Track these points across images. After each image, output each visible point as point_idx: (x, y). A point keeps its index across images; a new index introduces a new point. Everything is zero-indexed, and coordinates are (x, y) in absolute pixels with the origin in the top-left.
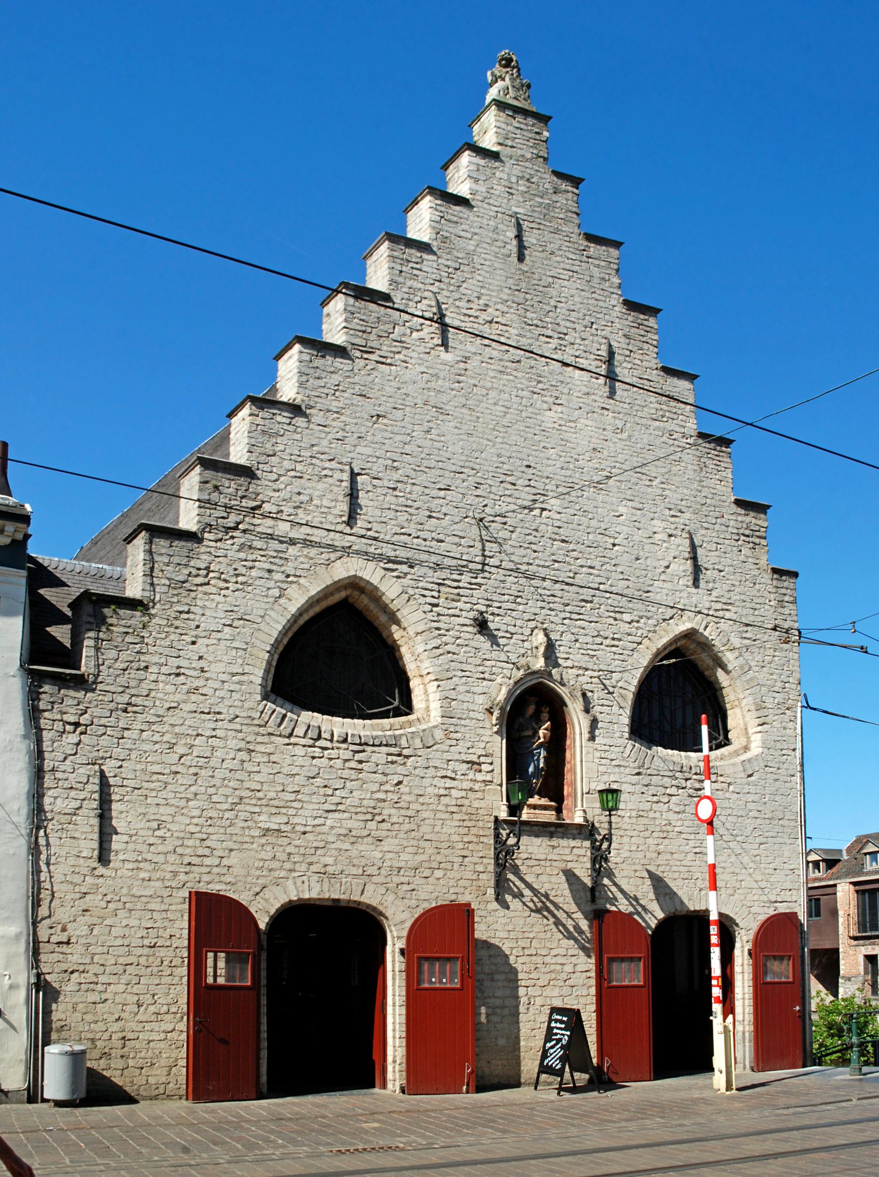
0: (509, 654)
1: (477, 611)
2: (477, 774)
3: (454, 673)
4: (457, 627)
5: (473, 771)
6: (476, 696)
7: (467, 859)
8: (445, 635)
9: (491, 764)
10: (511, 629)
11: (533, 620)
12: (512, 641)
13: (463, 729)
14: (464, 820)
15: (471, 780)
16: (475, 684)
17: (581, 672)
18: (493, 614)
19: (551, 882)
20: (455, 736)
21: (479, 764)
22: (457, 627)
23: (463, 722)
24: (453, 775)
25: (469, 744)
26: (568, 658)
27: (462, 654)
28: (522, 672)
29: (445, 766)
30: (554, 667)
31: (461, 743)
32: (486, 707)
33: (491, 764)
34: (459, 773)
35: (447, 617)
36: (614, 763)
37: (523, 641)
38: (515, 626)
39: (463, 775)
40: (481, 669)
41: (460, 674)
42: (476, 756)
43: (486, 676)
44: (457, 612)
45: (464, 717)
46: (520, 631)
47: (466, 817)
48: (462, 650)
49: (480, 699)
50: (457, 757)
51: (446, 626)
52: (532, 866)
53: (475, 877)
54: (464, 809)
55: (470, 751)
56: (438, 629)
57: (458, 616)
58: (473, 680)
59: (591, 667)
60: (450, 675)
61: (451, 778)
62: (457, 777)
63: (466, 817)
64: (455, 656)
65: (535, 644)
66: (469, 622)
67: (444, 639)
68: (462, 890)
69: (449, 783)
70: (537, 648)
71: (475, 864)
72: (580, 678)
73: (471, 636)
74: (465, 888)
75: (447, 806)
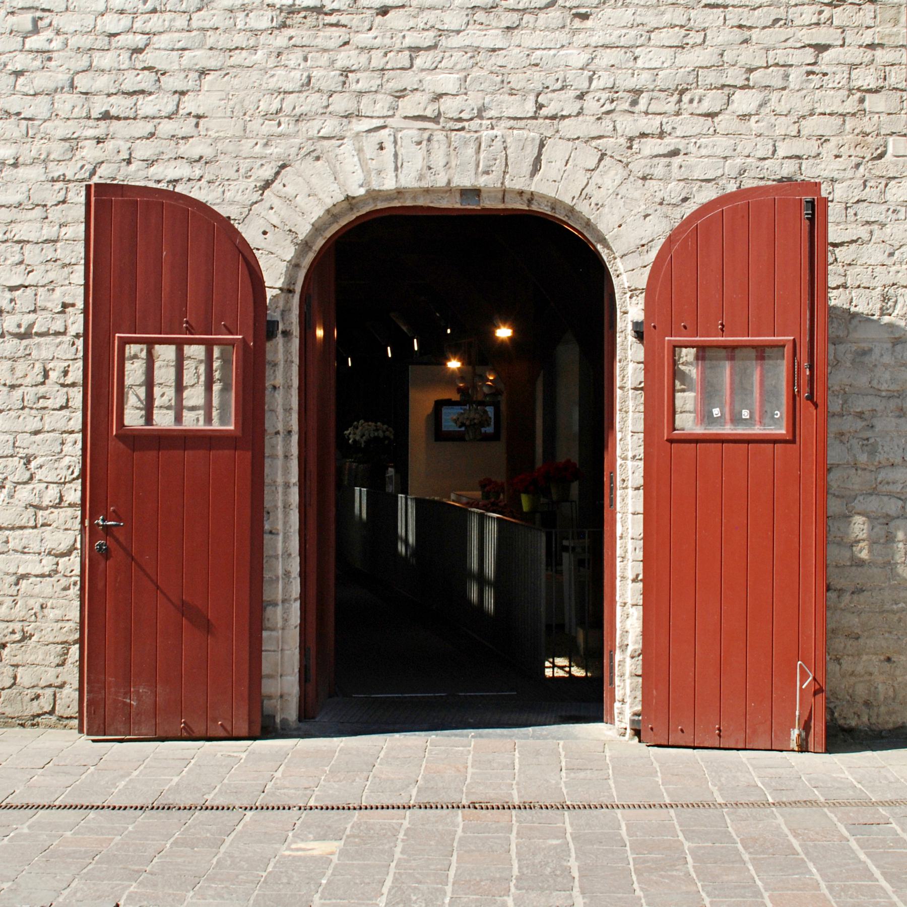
7: (827, 56)
53: (851, 105)
68: (812, 147)
71: (853, 66)
74: (823, 140)
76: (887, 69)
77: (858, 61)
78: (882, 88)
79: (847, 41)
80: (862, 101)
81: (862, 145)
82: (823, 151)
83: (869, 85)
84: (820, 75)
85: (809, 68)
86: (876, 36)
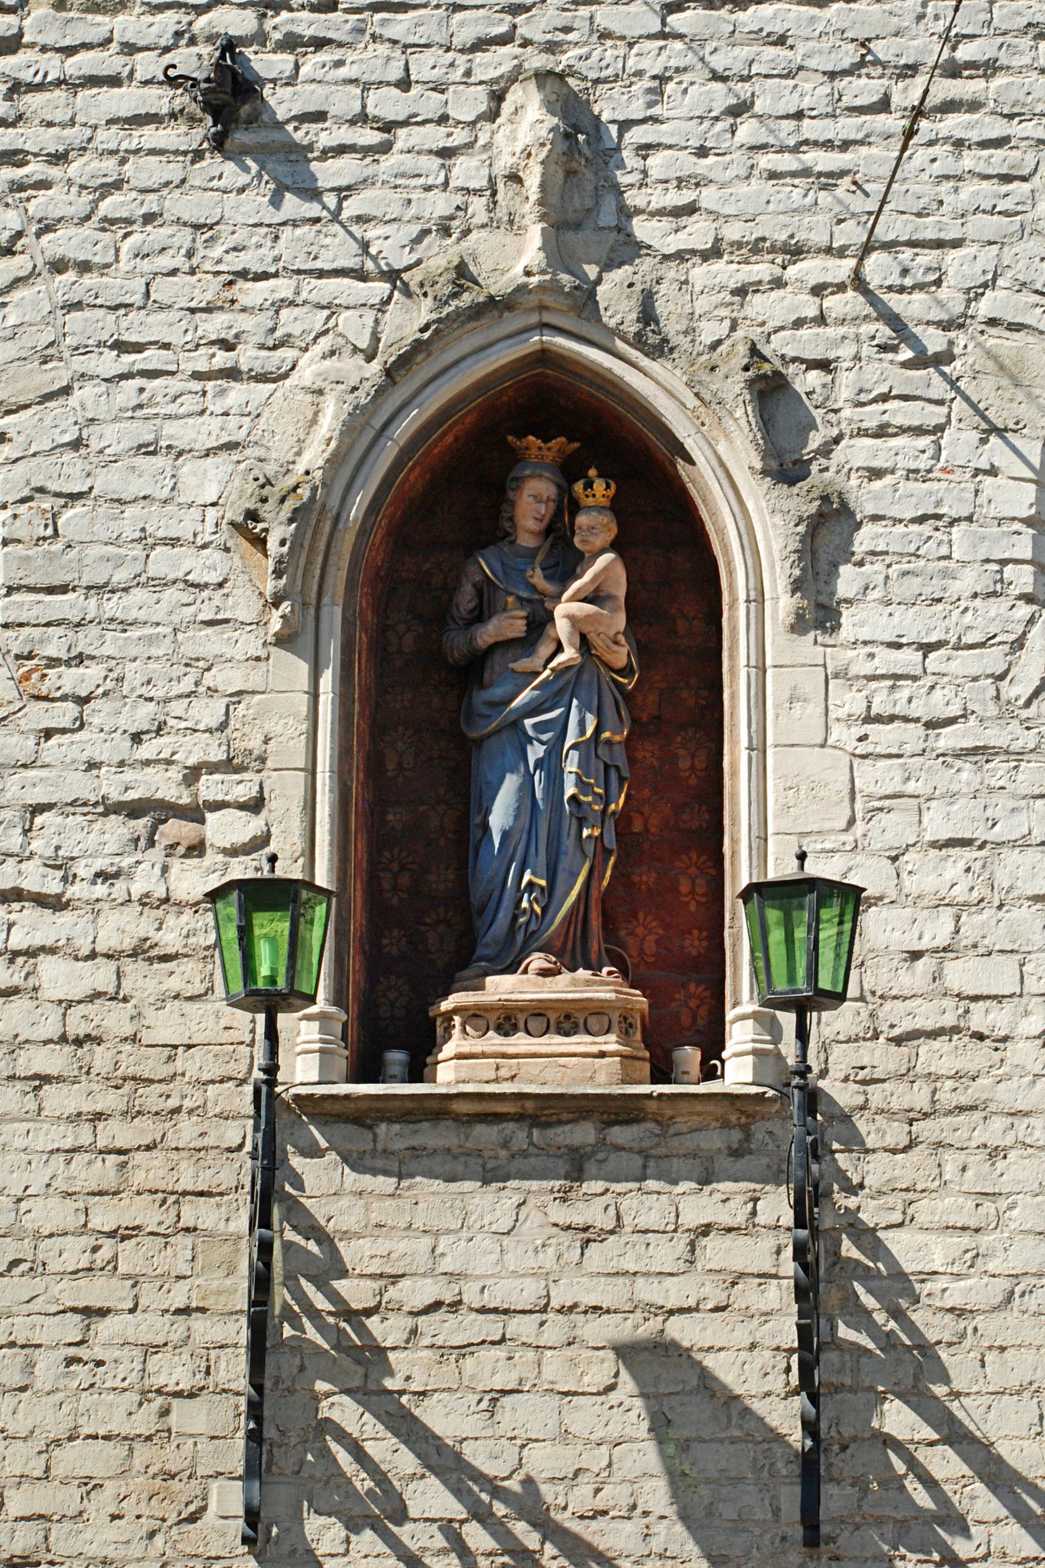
0: (372, 232)
1: (210, 39)
2: (176, 865)
3: (79, 364)
4: (109, 138)
5: (157, 854)
6: (188, 467)
7: (106, 1328)
8: (44, 185)
9: (255, 805)
11: (504, 40)
13: (112, 644)
14: (98, 1116)
15: (145, 901)
16: (190, 404)
17: (761, 270)
18: (291, 43)
20: (70, 679)
21: (195, 813)
22: (109, 138)
23: (113, 606)
24: (53, 886)
25: (143, 716)
26: (691, 209)
27: (124, 266)
28: (424, 312)
29: (14, 841)
30: (609, 265)
31: (99, 713)
32: (229, 516)
33: (255, 805)
34: (82, 870)
35: (60, 95)
36: (948, 739)
37: (446, 153)
38: (404, 84)
39: (102, 876)
40: (215, 325)
41: (109, 363)
42: (175, 774)
43: (246, 357)
44: (108, 62)
45: (121, 577)
46: (430, 104)
47: (110, 1100)
48: (126, 246)
50: (81, 786)
51: (50, 140)
52: (464, 1350)
53: (145, 1421)
55: (147, 750)
57: (114, 81)
58: (174, 385)
59: (819, 238)
60: (58, 375)
61: (41, 900)
62: (75, 891)
64: (90, 280)
65: (504, 163)
66: (160, 99)
67: (40, 203)
68: (69, 1499)
70: (514, 178)
71: (152, 1349)
72: (758, 305)
73: (173, 171)
74: (90, 1485)
76: (213, 1354)
77: (159, 1340)
78: (203, 1388)
79: (143, 1302)
80: (165, 1412)
81: (161, 1496)
82: (91, 1507)
83: (178, 1384)
84: (91, 1365)
85: (72, 1351)
86: (194, 1294)
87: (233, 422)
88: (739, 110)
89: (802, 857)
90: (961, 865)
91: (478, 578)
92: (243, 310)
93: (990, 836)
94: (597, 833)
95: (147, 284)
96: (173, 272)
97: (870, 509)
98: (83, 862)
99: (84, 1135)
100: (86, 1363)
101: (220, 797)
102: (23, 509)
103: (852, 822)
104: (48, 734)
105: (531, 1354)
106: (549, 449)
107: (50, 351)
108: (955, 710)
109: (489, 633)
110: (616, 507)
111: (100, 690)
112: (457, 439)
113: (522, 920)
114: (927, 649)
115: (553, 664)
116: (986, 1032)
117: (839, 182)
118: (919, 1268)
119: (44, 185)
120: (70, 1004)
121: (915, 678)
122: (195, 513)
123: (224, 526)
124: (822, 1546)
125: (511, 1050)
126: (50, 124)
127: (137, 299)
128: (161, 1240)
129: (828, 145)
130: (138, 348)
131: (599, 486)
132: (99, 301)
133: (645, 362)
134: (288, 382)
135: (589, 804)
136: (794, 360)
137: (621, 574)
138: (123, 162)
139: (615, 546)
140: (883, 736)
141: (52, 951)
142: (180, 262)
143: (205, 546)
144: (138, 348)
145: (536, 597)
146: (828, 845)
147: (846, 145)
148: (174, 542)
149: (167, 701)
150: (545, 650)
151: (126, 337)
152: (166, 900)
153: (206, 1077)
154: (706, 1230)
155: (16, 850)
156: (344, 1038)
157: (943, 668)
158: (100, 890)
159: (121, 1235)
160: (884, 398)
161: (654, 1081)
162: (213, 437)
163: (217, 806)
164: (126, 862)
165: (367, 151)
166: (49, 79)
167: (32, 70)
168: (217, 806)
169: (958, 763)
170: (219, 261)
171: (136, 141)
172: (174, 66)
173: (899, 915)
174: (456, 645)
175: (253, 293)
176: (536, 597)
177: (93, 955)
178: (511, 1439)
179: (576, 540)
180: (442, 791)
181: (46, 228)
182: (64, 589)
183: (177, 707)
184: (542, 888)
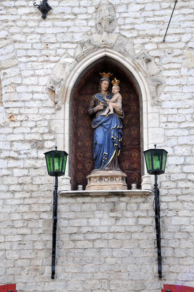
3: (20, 60)
4: (24, 17)
6: (41, 79)
7: (27, 237)
8: (12, 26)
9: (53, 140)
10: (76, 10)
12: (77, 22)
13: (27, 111)
14: (25, 198)
16: (40, 67)
17: (147, 40)
19: (113, 257)
20: (19, 118)
22: (24, 17)
23: (27, 104)
24: (16, 155)
25: (32, 124)
26: (133, 29)
34: (22, 152)
36: (183, 125)
37: (86, 19)
38: (79, 6)
43: (52, 58)
49: (45, 81)
50: (21, 137)
52: (94, 241)
54: (26, 187)
55: (34, 130)
56: (7, 21)
60: (15, 62)
63: (27, 195)
67: (12, 30)
69: (12, 163)
71: (34, 241)
75: (9, 185)
76: (46, 242)
77: (36, 239)
79: (33, 232)
80: (37, 253)
81: (36, 270)
82: (23, 273)
83: (39, 248)
84: (23, 245)
85: (19, 242)
86: (42, 231)
87: (48, 70)
88: (143, 10)
89: (155, 146)
90: (186, 149)
91: (94, 99)
92: (50, 49)
93: (190, 143)
94: (117, 145)
95: (32, 45)
96: (37, 42)
97: (167, 83)
98: (22, 151)
99: (22, 202)
100: (22, 244)
101: (47, 139)
102: (9, 87)
103: (165, 141)
104: (14, 128)
105: (106, 241)
106: (107, 75)
107: (14, 57)
108: (184, 120)
109: (96, 109)
110: (119, 85)
111: (24, 120)
112: (90, 74)
113: (103, 161)
114: (178, 109)
115: (108, 114)
116: (191, 180)
117: (161, 23)
118: (179, 224)
119: (12, 26)
120: (20, 177)
121: (176, 114)
122: (42, 87)
123: (47, 89)
124: (162, 277)
125: (102, 184)
126: (12, 15)
127: (30, 48)
128: (36, 221)
129: (159, 16)
130: (30, 57)
131: (117, 81)
132: (23, 48)
133: (125, 58)
134: (59, 63)
135: (115, 139)
136: (152, 56)
137: (120, 97)
138: (27, 22)
139: (119, 92)
140: (170, 125)
141: (16, 168)
142: (38, 41)
143: (43, 93)
144: (30, 57)
145: (105, 102)
146: (160, 145)
147: (162, 16)
148: (37, 92)
149: (37, 121)
150: (107, 111)
151: (28, 55)
152: (37, 158)
153: (44, 190)
154: (139, 217)
155: (9, 149)
156: (70, 182)
157: (181, 112)
158: (25, 156)
159: (29, 220)
160: (170, 63)
161: (128, 189)
162: (45, 73)
163: (47, 140)
164: (29, 151)
165: (73, 19)
166: (12, 6)
167: (9, 4)
168: (47, 140)
169: (184, 130)
170: (46, 40)
171: (29, 18)
172: (35, 3)
173: (174, 158)
174: (91, 110)
175: (51, 47)
176: (105, 102)
177: (24, 168)
178: (102, 257)
179: (113, 91)
180: (88, 139)
181: (12, 34)
182: (17, 101)
183: (39, 123)
184: (107, 155)
